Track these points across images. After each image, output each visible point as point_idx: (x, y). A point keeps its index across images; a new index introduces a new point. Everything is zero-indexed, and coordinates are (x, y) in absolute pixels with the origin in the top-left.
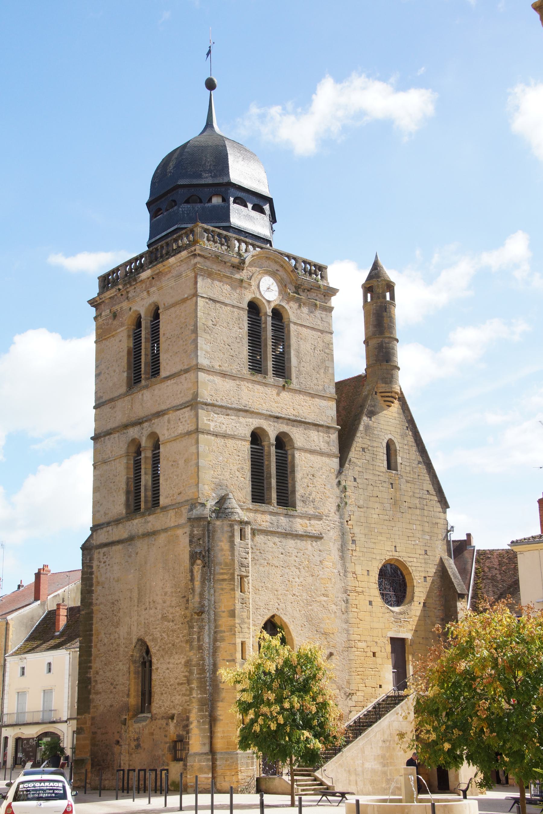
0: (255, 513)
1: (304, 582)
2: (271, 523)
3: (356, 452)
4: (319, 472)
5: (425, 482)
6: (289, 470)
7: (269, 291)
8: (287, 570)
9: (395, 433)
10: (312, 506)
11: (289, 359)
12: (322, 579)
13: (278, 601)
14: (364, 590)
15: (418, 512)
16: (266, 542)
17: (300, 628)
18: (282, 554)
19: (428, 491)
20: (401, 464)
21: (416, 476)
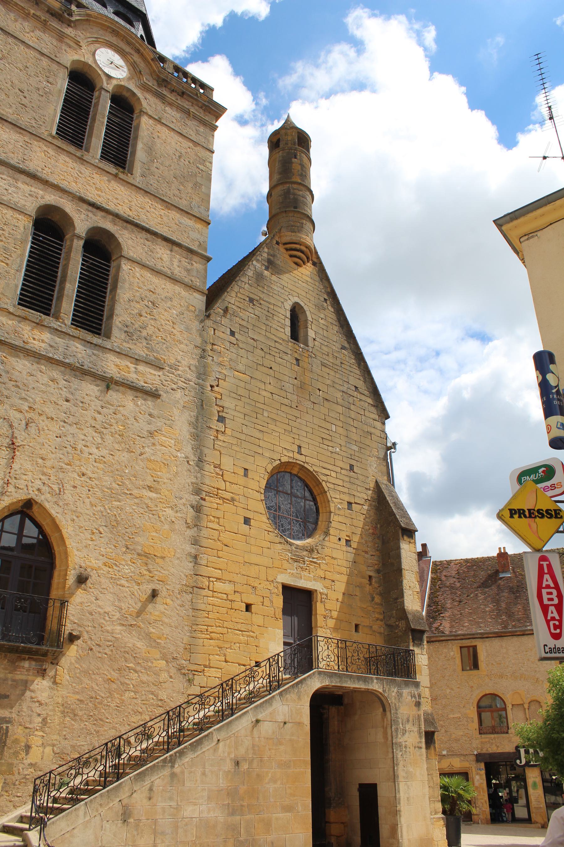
0: (19, 322)
1: (109, 458)
2: (51, 346)
3: (237, 299)
4: (166, 302)
5: (352, 374)
6: (109, 288)
7: (111, 65)
8: (73, 429)
9: (305, 299)
10: (145, 344)
11: (134, 153)
12: (149, 460)
13: (43, 477)
14: (237, 497)
15: (340, 409)
16: (34, 373)
17: (89, 536)
18: (67, 401)
19: (356, 387)
20: (314, 339)
21: (338, 362)
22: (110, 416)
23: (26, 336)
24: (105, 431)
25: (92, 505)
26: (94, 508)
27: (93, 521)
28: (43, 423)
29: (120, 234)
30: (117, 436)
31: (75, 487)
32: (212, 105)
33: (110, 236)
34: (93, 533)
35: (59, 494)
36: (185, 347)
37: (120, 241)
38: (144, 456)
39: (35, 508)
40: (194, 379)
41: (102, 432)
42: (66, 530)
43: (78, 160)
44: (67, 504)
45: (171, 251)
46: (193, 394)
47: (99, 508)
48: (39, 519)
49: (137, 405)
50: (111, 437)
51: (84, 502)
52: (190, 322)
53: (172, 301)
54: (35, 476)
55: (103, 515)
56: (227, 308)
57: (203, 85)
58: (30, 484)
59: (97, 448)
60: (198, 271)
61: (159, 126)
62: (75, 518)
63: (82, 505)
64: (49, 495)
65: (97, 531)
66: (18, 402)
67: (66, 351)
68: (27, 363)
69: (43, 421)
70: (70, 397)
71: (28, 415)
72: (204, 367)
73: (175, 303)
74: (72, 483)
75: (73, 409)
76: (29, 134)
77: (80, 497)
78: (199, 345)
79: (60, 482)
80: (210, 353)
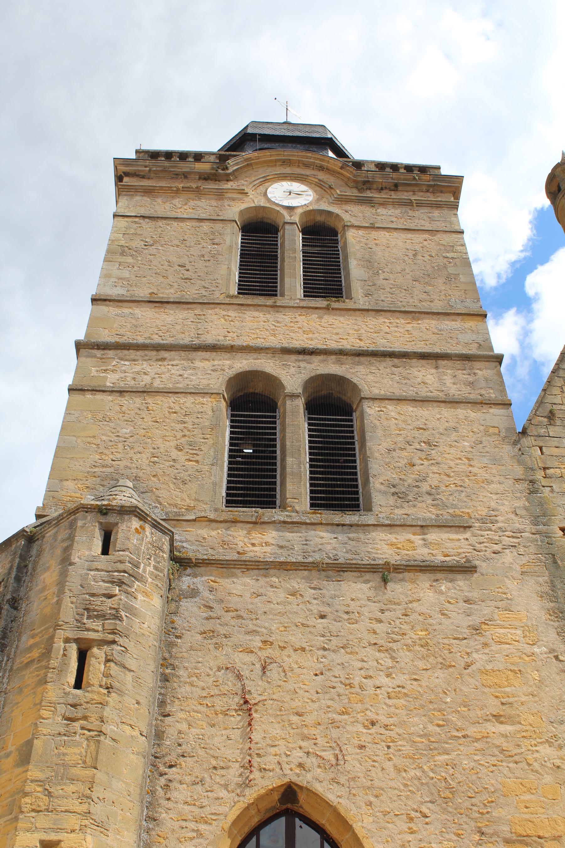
0: (227, 529)
1: (411, 686)
2: (281, 547)
4: (448, 436)
6: (357, 446)
8: (341, 657)
10: (430, 501)
12: (485, 672)
13: (303, 744)
16: (261, 591)
17: (405, 827)
18: (322, 617)
22: (398, 622)
23: (241, 544)
24: (394, 646)
25: (398, 770)
26: (404, 774)
27: (407, 797)
28: (289, 659)
29: (353, 373)
30: (417, 648)
31: (362, 747)
32: (439, 181)
33: (341, 381)
34: (411, 819)
35: (337, 765)
36: (498, 486)
37: (355, 381)
38: (474, 667)
39: (302, 797)
40: (529, 527)
41: (391, 649)
42: (360, 824)
43: (270, 309)
44: (353, 779)
45: (437, 368)
46: (533, 549)
47: (412, 773)
48: (316, 817)
49: (441, 593)
50: (408, 653)
51: (383, 769)
52: (497, 449)
53: (457, 431)
54: (290, 745)
55: (422, 784)
56: (551, 412)
57: (423, 169)
58: (284, 759)
59: (388, 676)
60: (486, 380)
61: (373, 233)
62: (372, 799)
63: (380, 774)
64: (319, 770)
65: (418, 814)
66: (242, 638)
67: (305, 546)
68: (248, 580)
69: (289, 656)
70: (325, 609)
71: (263, 654)
72: (541, 504)
73: (463, 431)
74: (356, 742)
75: (335, 627)
76: (200, 306)
77: (374, 761)
78: (522, 477)
79: (334, 745)
80: (544, 482)
